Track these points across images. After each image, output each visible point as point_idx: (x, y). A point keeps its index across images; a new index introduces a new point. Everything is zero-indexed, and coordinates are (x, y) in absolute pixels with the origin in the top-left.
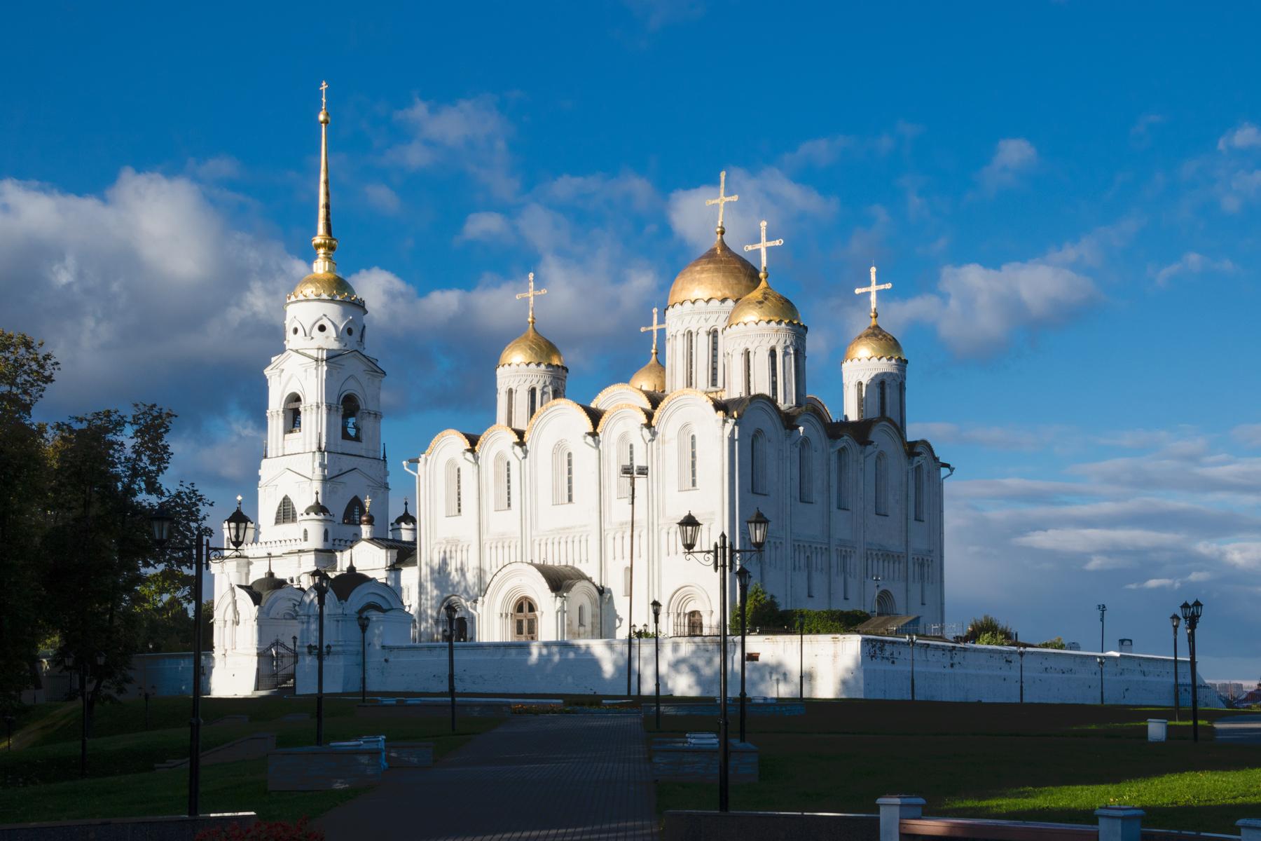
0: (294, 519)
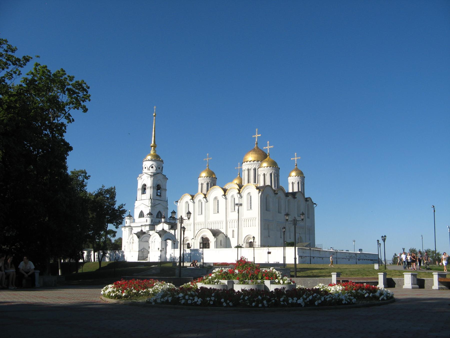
0: (144, 217)
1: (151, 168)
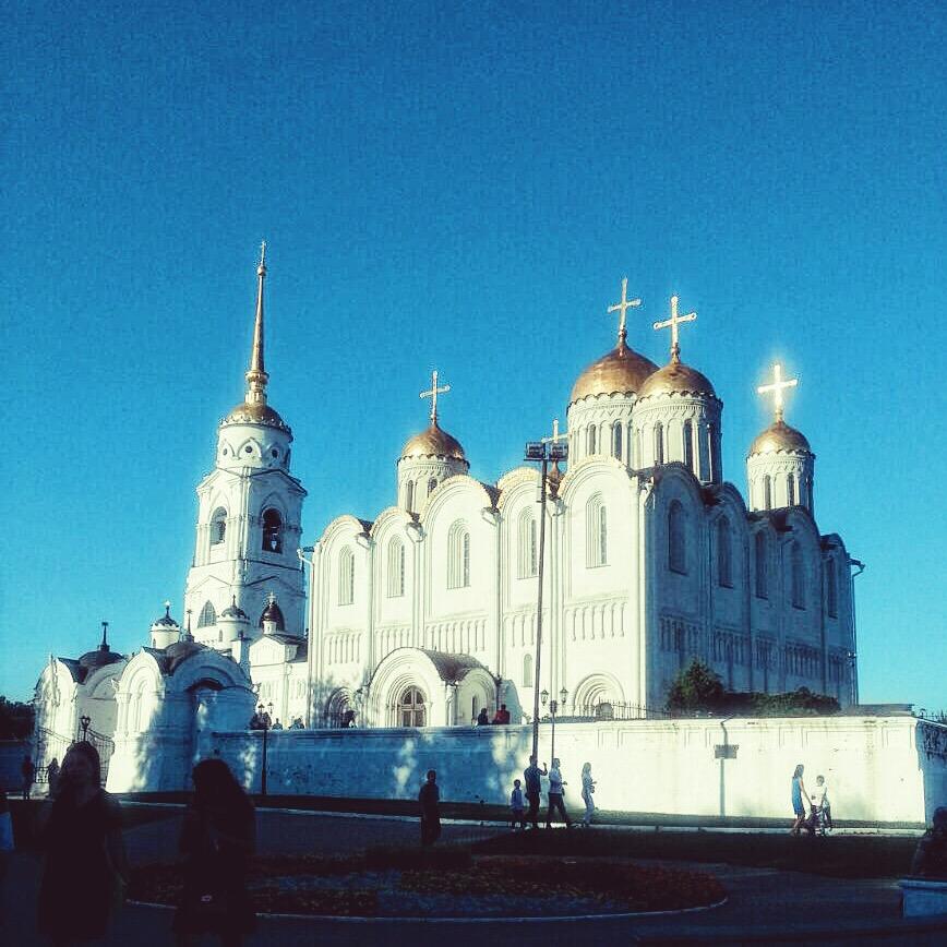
1: (243, 453)
